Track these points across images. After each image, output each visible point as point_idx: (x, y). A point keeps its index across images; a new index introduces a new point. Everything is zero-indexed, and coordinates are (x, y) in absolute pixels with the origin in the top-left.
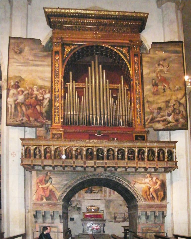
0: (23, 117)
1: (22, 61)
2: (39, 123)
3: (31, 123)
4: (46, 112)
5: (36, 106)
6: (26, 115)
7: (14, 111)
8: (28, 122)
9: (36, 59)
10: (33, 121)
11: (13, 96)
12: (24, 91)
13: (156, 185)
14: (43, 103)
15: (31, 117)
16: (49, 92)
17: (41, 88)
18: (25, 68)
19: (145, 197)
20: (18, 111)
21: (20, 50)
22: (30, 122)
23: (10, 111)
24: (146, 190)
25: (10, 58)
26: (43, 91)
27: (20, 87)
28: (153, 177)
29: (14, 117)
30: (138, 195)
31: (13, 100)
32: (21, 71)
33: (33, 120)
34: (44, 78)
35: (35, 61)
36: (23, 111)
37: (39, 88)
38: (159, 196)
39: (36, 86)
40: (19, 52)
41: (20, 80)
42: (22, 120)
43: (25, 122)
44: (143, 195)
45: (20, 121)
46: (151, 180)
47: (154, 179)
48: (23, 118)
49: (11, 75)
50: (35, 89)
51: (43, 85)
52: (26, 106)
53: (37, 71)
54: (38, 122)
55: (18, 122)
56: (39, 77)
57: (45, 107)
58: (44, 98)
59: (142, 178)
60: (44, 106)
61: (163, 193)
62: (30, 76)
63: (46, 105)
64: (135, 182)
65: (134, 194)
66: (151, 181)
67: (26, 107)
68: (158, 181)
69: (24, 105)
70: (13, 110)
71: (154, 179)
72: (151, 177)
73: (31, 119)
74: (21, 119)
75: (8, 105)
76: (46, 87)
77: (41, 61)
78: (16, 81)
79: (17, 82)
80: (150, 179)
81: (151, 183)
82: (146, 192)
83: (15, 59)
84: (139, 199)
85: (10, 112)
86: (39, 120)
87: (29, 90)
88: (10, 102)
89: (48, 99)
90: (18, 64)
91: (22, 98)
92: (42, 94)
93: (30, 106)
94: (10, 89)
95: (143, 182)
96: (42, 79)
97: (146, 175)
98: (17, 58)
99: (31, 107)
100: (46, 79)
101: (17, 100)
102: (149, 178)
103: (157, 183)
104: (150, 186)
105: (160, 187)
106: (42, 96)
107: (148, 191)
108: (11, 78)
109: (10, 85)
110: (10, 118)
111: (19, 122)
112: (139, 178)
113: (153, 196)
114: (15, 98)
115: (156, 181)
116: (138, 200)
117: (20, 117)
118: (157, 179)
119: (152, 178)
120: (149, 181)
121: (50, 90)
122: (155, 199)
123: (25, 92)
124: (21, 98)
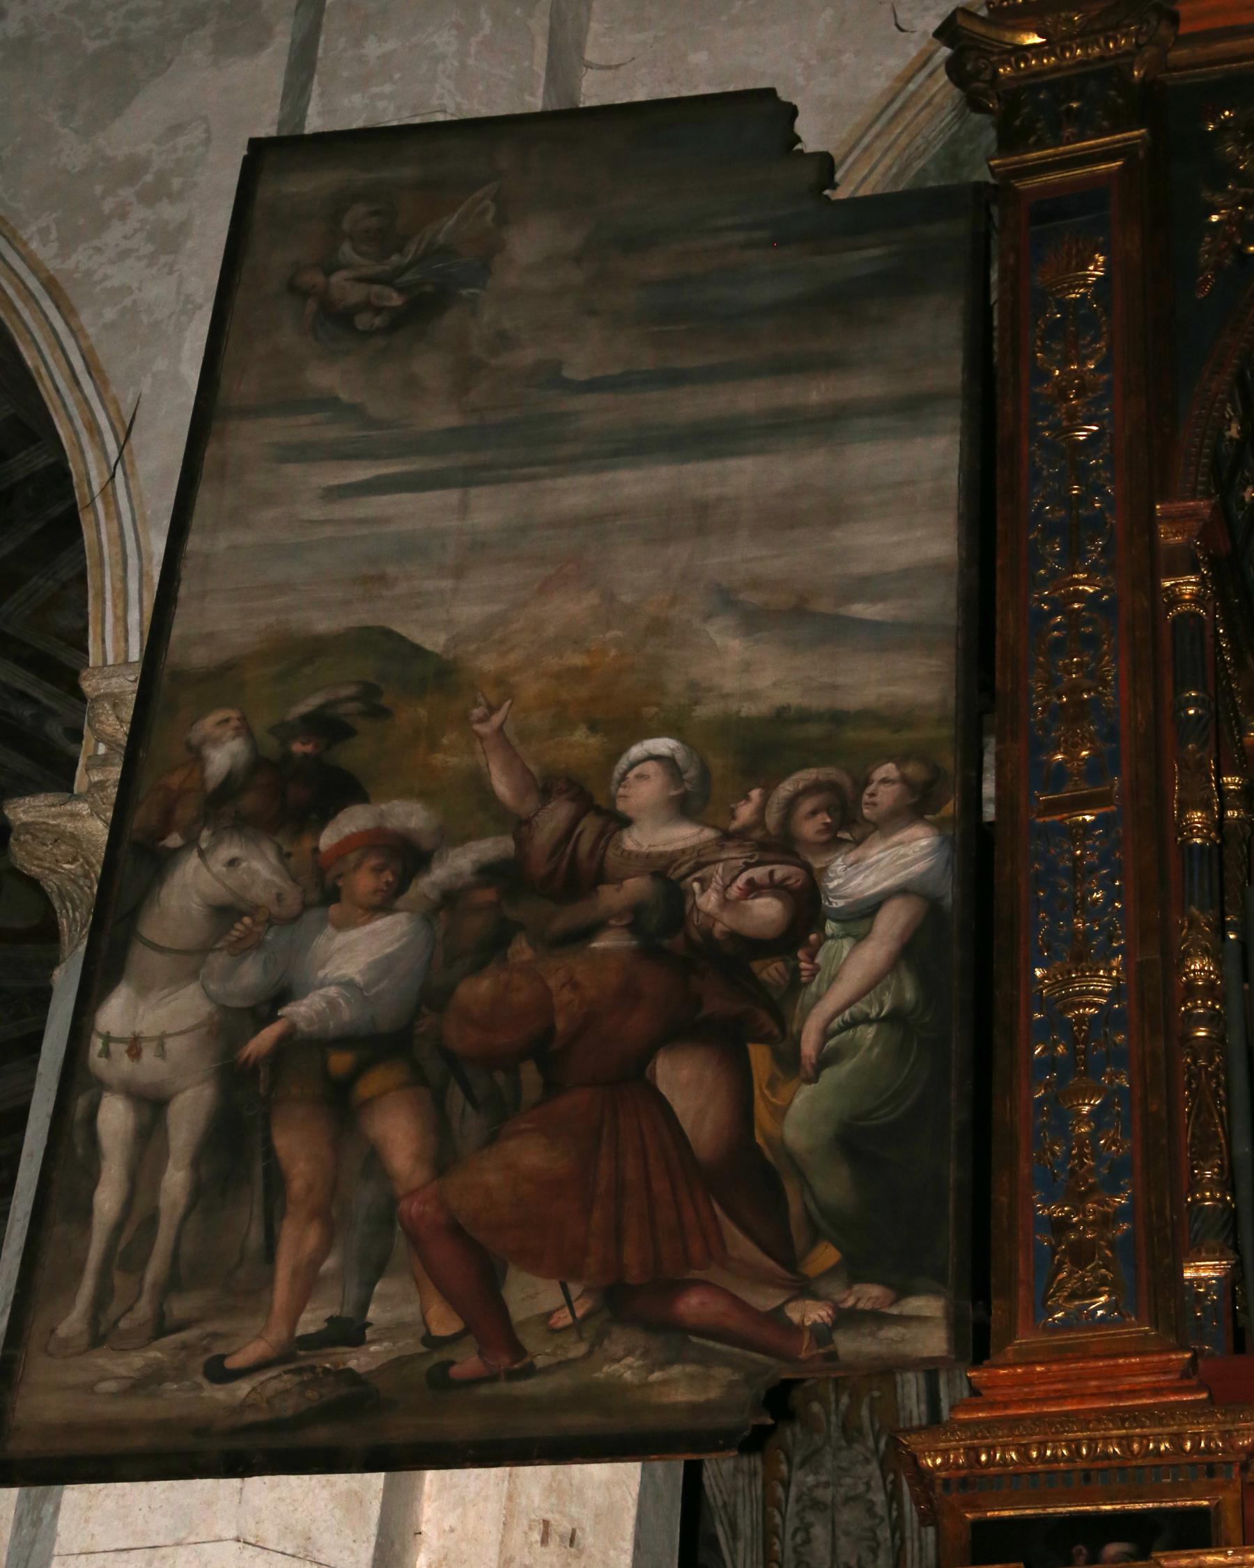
0: (375, 1268)
1: (441, 417)
2: (707, 1358)
3: (529, 1371)
4: (854, 1141)
5: (646, 1057)
6: (415, 1240)
7: (198, 1191)
8: (467, 1362)
9: (689, 360)
10: (578, 1326)
11: (205, 950)
12: (426, 843)
14: (795, 984)
15: (534, 1262)
16: (918, 805)
17: (762, 747)
18: (489, 509)
20: (275, 1182)
21: (408, 277)
22: (504, 1361)
23: (107, 1200)
25: (247, 412)
26: (791, 803)
27: (363, 798)
29: (180, 1307)
31: (206, 1008)
32: (412, 548)
33: (563, 1319)
34: (824, 605)
35: (674, 378)
36: (374, 1160)
37: (717, 764)
39: (663, 745)
40: (396, 300)
41: (369, 692)
42: (348, 1331)
43: (399, 1363)
45: (288, 1354)
48: (364, 1307)
49: (218, 622)
50: (643, 791)
51: (818, 702)
52: (456, 1097)
53: (703, 518)
54: (673, 1337)
55: (243, 1388)
56: (726, 599)
57: (826, 1060)
58: (807, 907)
60: (809, 1046)
62: (569, 608)
63: (866, 1020)
67: (440, 1099)
69: (418, 1078)
70: (175, 1181)
73: (531, 1296)
74: (311, 1321)
75: (81, 1104)
76: (851, 734)
77: (782, 368)
78: (313, 702)
79: (327, 726)
83: (325, 403)
85: (118, 1228)
86: (692, 1304)
87: (520, 827)
88: (134, 1046)
89: (891, 924)
90: (361, 473)
91: (384, 966)
92: (781, 845)
93: (530, 1073)
94: (174, 840)
96: (795, 616)
98: (344, 396)
99: (552, 1087)
100: (862, 610)
101: (283, 995)
106: (780, 871)
108: (221, 682)
109: (175, 780)
110: (99, 1336)
111: (275, 1381)
114: (251, 975)
117: (309, 1283)
121: (949, 761)
123: (458, 863)
124: (356, 958)
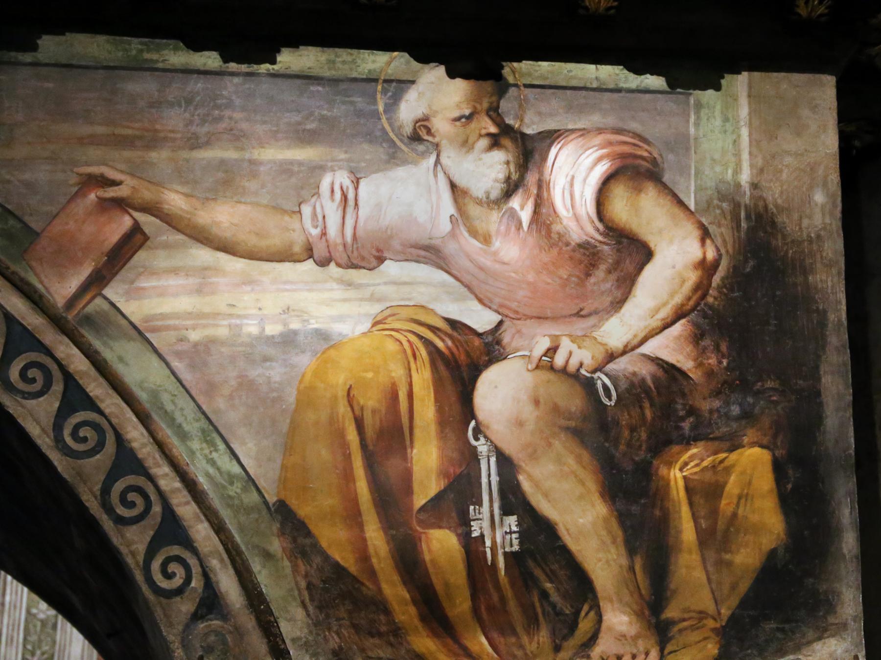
13: (618, 304)
19: (364, 557)
24: (371, 401)
28: (551, 136)
30: (187, 510)
38: (687, 530)
44: (304, 511)
46: (511, 188)
47: (575, 173)
59: (305, 137)
61: (778, 467)
64: (126, 222)
65: (86, 475)
66: (493, 221)
68: (644, 212)
71: (575, 173)
72: (495, 142)
80: (487, 169)
81: (510, 250)
82: (388, 437)
84: (211, 602)
95: (322, 217)
97: (399, 86)
102: (451, 158)
103: (628, 252)
104: (481, 319)
105: (697, 337)
107: (426, 411)
112: (237, 138)
113: (539, 534)
115: (621, 207)
116: (185, 607)
118: (634, 170)
119: (529, 151)
120: (448, 207)
122: (582, 586)
